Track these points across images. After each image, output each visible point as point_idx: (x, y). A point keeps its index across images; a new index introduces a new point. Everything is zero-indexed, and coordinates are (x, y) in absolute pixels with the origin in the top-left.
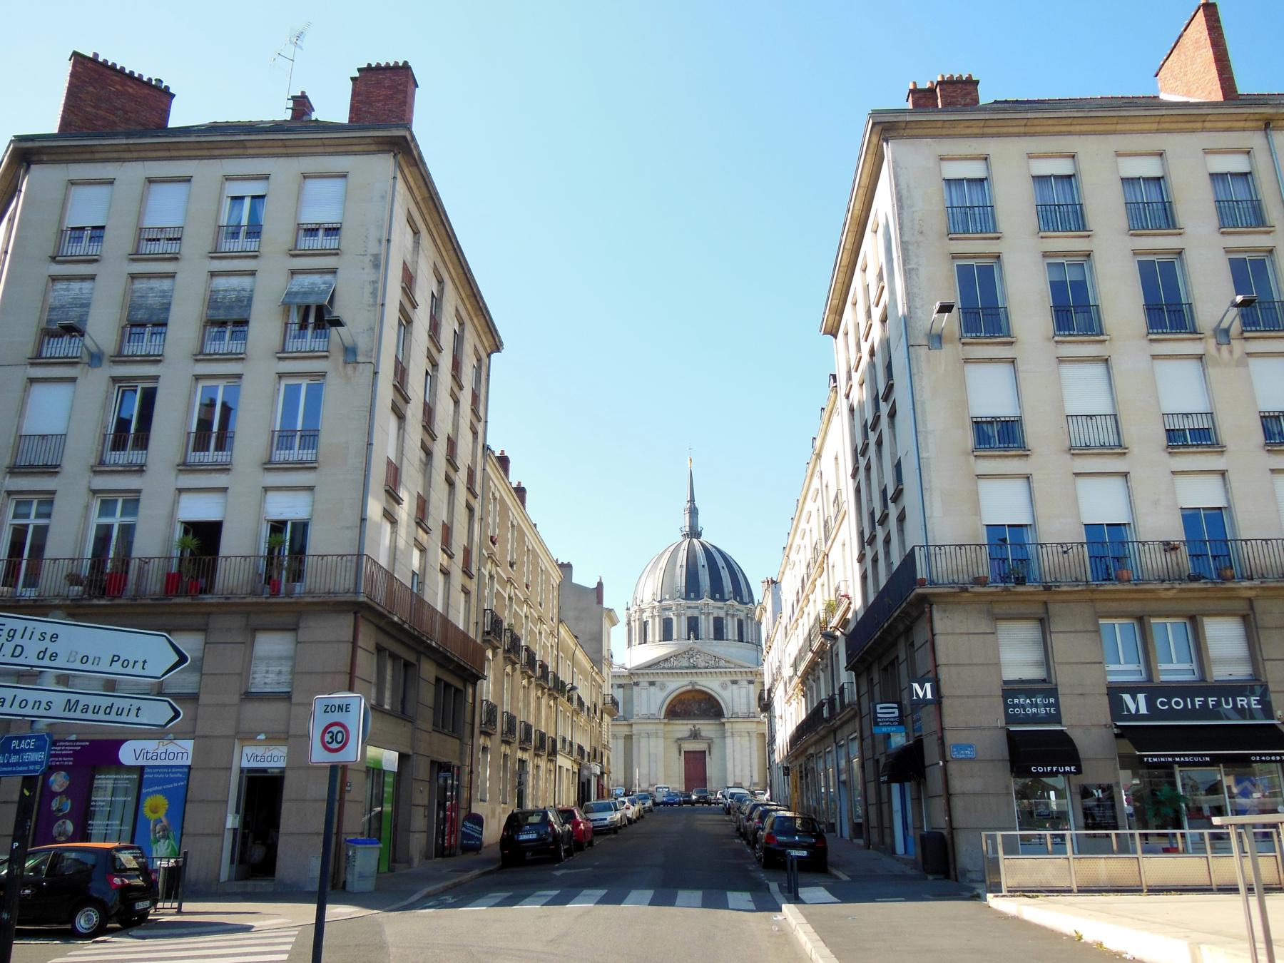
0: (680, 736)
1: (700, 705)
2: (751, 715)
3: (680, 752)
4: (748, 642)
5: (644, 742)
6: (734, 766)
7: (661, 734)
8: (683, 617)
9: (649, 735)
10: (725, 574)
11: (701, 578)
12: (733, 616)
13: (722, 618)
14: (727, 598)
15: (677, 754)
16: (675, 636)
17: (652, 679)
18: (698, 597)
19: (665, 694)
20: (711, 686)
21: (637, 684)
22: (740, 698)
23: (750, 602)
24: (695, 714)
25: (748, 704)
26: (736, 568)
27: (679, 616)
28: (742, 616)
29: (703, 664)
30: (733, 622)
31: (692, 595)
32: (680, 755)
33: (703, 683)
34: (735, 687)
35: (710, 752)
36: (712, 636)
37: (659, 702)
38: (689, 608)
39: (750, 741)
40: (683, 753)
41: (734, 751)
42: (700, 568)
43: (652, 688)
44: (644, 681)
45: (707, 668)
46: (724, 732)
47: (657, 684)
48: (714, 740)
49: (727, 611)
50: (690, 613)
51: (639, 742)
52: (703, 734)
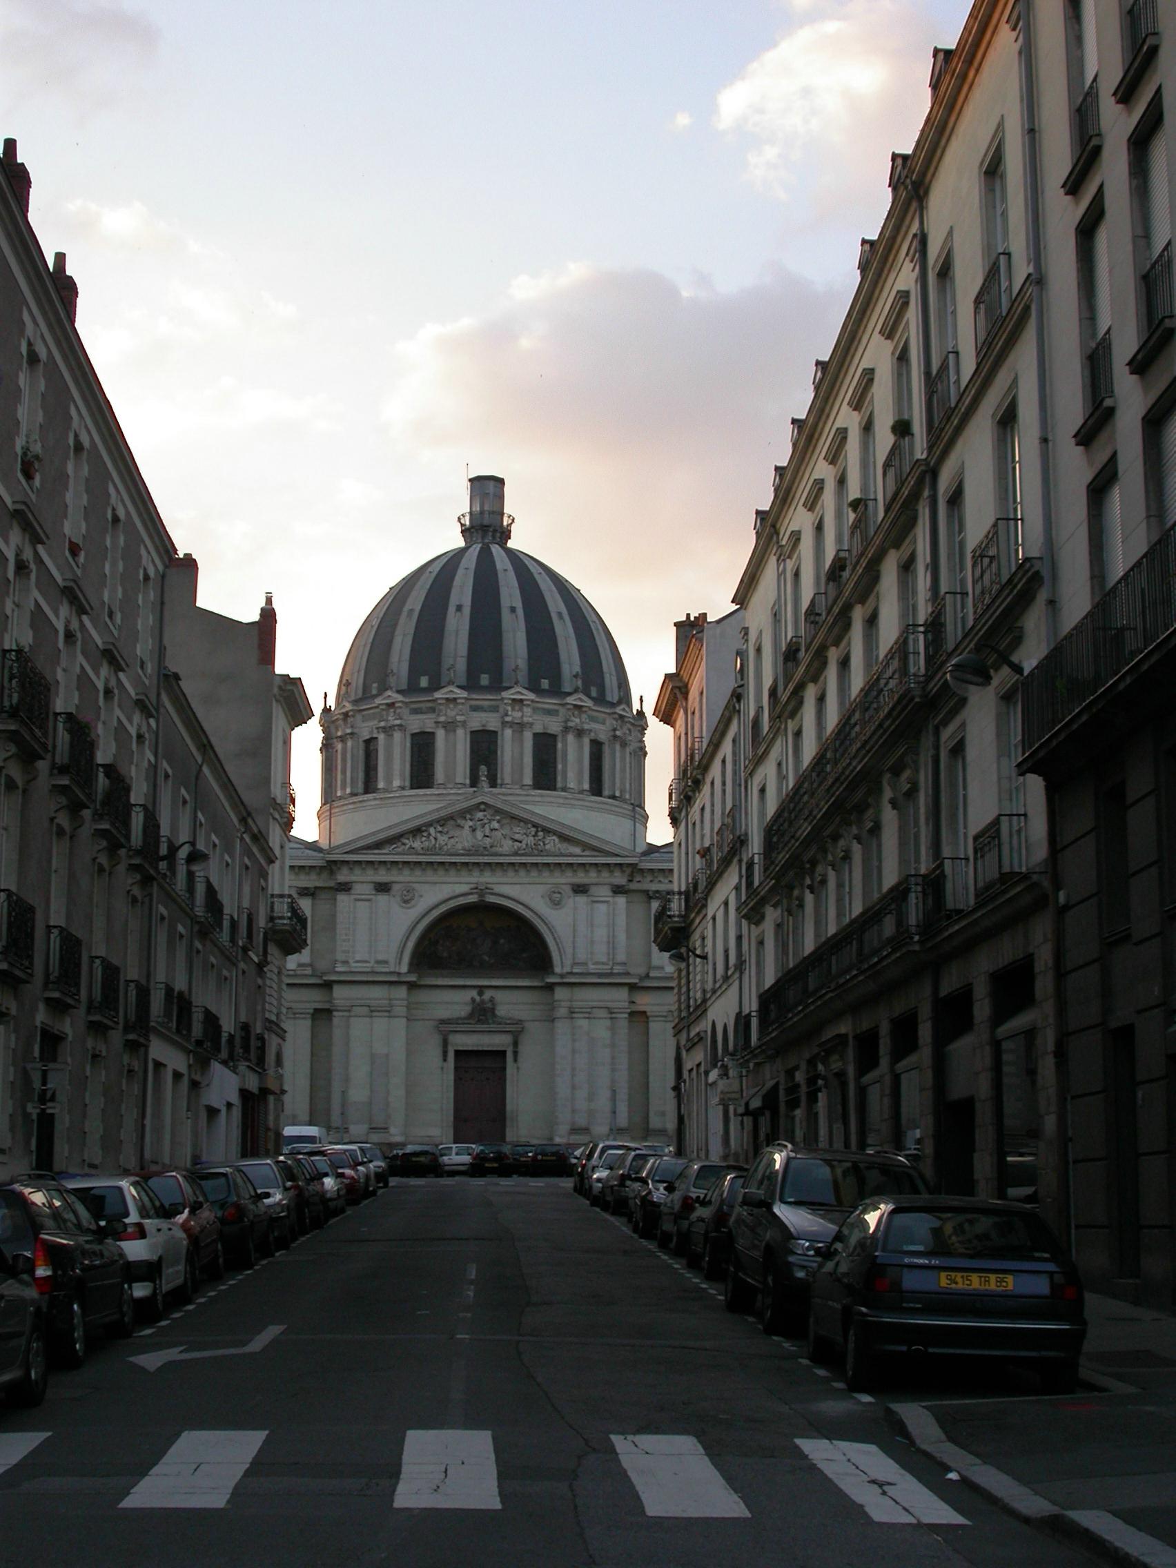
0: (444, 1013)
2: (617, 969)
3: (445, 1053)
4: (613, 797)
5: (358, 1026)
6: (574, 1087)
7: (401, 1011)
8: (460, 732)
9: (373, 1011)
10: (564, 631)
11: (507, 637)
12: (580, 733)
13: (554, 737)
14: (568, 690)
15: (438, 1052)
16: (440, 775)
17: (382, 876)
18: (497, 685)
20: (523, 898)
21: (345, 888)
22: (591, 925)
23: (620, 702)
25: (612, 943)
26: (591, 618)
28: (602, 731)
29: (507, 846)
30: (581, 747)
31: (485, 680)
32: (445, 1060)
33: (506, 890)
34: (581, 900)
36: (528, 779)
37: (400, 930)
38: (475, 709)
39: (612, 1029)
40: (451, 1055)
41: (574, 1051)
43: (382, 899)
44: (363, 881)
45: (516, 854)
46: (552, 1007)
47: (396, 887)
48: (526, 1025)
49: (567, 721)
50: (477, 721)
51: (348, 1027)
52: (501, 1011)
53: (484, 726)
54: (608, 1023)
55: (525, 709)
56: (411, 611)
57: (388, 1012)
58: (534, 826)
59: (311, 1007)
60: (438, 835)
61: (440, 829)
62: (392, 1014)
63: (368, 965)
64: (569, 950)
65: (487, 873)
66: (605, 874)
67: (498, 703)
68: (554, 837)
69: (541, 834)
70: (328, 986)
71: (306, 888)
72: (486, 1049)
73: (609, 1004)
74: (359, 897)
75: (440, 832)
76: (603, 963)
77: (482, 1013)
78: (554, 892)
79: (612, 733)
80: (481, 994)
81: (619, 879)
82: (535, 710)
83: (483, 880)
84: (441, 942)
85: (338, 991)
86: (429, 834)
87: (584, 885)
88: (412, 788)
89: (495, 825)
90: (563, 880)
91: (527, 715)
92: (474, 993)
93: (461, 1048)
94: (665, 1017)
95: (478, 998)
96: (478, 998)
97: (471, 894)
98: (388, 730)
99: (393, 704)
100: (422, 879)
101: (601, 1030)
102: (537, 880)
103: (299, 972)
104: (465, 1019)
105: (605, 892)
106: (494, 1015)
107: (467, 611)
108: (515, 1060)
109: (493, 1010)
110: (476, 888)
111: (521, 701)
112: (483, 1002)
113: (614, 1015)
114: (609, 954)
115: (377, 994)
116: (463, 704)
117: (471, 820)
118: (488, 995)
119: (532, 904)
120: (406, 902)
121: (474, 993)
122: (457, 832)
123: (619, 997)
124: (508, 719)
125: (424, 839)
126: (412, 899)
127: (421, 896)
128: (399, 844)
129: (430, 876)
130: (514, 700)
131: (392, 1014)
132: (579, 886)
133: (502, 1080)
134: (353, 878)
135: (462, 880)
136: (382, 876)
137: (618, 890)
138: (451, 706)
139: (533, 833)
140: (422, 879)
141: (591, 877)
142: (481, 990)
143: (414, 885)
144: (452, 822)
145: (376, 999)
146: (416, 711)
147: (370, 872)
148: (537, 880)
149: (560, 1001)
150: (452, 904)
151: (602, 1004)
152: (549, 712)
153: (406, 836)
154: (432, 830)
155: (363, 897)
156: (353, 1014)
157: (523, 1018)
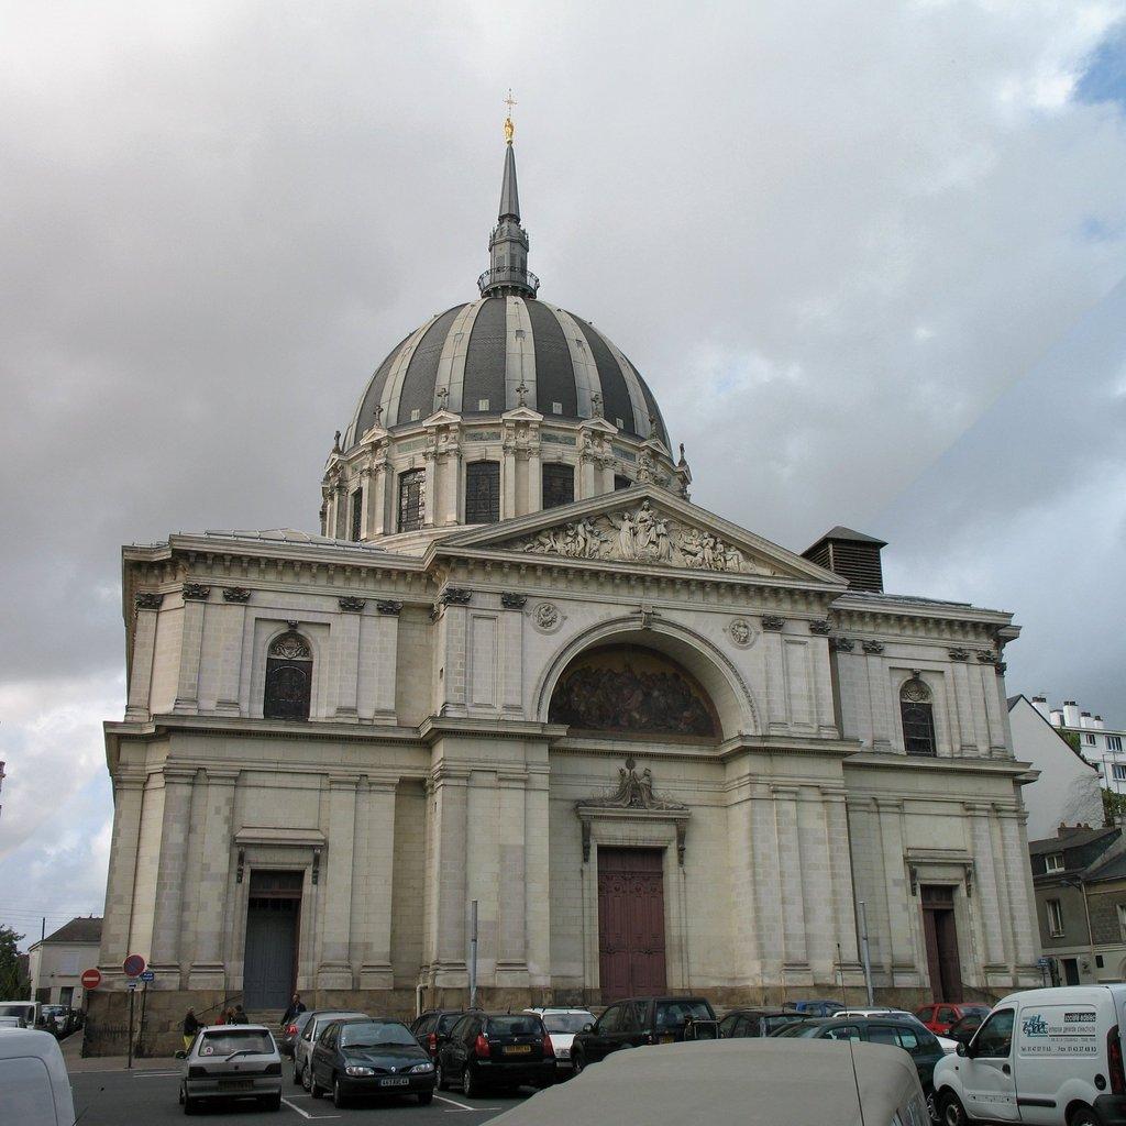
0: (584, 792)
1: (647, 695)
6: (783, 902)
7: (541, 781)
9: (504, 779)
15: (577, 848)
17: (513, 585)
20: (700, 630)
22: (787, 673)
24: (632, 724)
31: (557, 408)
32: (586, 860)
34: (774, 638)
35: (681, 851)
38: (547, 438)
42: (573, 346)
43: (513, 618)
51: (466, 802)
52: (661, 790)
54: (819, 808)
55: (606, 445)
57: (526, 785)
59: (395, 775)
60: (588, 535)
61: (589, 528)
63: (491, 711)
64: (763, 706)
65: (654, 594)
66: (801, 607)
68: (738, 552)
69: (720, 546)
70: (427, 744)
71: (391, 603)
72: (640, 844)
73: (822, 782)
75: (591, 532)
76: (805, 725)
77: (635, 793)
78: (739, 626)
80: (630, 765)
81: (818, 613)
83: (645, 601)
84: (576, 689)
85: (441, 750)
88: (467, 523)
89: (661, 529)
91: (606, 451)
93: (606, 843)
94: (867, 805)
95: (627, 771)
96: (627, 771)
97: (633, 619)
98: (438, 457)
99: (447, 426)
101: (815, 819)
103: (376, 722)
104: (615, 799)
105: (802, 629)
106: (651, 797)
107: (530, 336)
108: (681, 862)
109: (649, 787)
111: (603, 433)
112: (634, 777)
113: (826, 798)
114: (811, 712)
115: (508, 754)
116: (536, 430)
119: (712, 639)
120: (544, 624)
121: (622, 764)
123: (831, 772)
124: (589, 451)
125: (569, 539)
126: (552, 621)
127: (565, 618)
128: (536, 543)
129: (577, 591)
130: (594, 431)
131: (529, 786)
132: (769, 618)
133: (658, 891)
134: (473, 586)
135: (621, 599)
136: (513, 585)
137: (817, 629)
139: (711, 544)
140: (565, 594)
141: (783, 609)
142: (631, 758)
143: (554, 602)
144: (605, 521)
145: (510, 762)
146: (475, 437)
148: (715, 608)
151: (811, 782)
152: (627, 455)
154: (580, 528)
155: (484, 613)
157: (688, 803)
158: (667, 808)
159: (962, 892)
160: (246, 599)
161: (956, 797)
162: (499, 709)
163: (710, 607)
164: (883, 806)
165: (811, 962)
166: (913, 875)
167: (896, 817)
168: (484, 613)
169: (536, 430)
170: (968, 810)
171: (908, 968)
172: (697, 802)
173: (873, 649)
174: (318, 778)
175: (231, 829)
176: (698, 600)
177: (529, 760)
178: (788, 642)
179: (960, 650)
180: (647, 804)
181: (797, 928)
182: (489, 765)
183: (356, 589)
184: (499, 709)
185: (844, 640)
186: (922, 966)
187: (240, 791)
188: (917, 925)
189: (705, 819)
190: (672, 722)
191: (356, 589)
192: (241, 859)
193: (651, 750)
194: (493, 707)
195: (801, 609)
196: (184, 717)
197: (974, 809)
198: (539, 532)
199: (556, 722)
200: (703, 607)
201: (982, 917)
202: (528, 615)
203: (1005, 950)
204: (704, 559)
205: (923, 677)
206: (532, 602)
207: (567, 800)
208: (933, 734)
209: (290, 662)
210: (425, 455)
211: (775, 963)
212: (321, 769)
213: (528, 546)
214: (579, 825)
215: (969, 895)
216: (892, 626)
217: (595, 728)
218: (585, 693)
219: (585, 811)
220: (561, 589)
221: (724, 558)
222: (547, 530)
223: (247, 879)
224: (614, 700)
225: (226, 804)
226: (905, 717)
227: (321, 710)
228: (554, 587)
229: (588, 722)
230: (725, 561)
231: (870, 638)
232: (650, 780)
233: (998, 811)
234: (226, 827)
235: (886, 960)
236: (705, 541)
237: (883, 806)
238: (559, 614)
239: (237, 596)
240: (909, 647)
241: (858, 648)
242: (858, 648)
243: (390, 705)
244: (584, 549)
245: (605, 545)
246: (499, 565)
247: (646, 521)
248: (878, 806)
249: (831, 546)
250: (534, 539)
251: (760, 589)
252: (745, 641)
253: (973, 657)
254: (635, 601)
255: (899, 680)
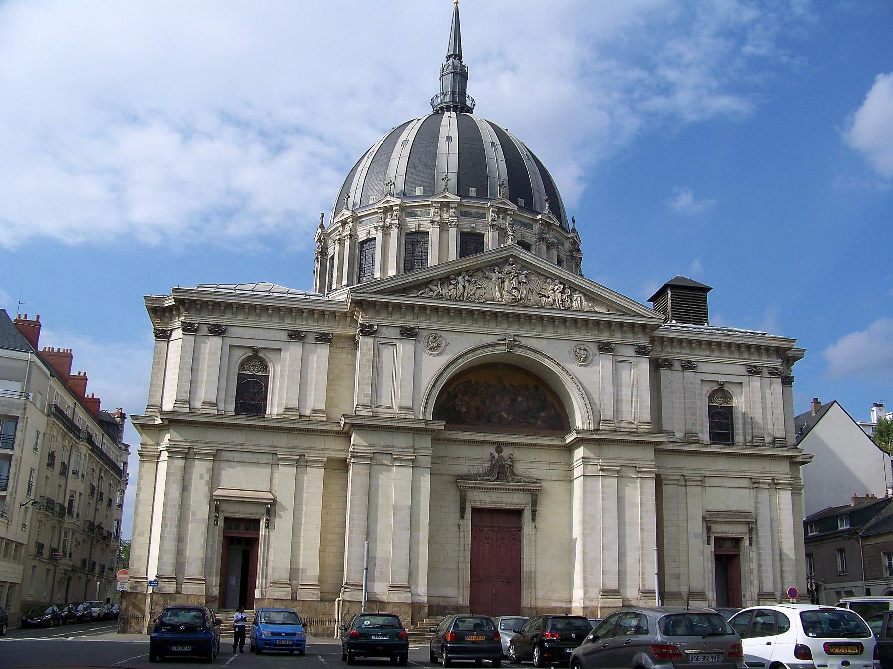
0: (464, 470)
7: (426, 461)
15: (455, 509)
17: (409, 321)
19: (441, 361)
27: (443, 227)
29: (534, 298)
31: (473, 192)
32: (462, 517)
38: (464, 214)
42: (488, 147)
44: (389, 324)
52: (521, 468)
53: (473, 228)
56: (407, 141)
58: (561, 284)
60: (467, 284)
61: (467, 278)
62: (417, 465)
67: (486, 211)
68: (581, 295)
69: (568, 292)
72: (504, 507)
74: (383, 341)
75: (468, 281)
76: (628, 422)
78: (580, 349)
79: (568, 254)
82: (515, 222)
83: (508, 331)
84: (460, 396)
86: (458, 283)
87: (609, 344)
90: (589, 338)
92: (492, 450)
93: (478, 506)
94: (678, 480)
95: (496, 455)
96: (496, 455)
97: (499, 345)
99: (392, 206)
100: (448, 327)
102: (564, 336)
103: (314, 419)
104: (485, 474)
106: (513, 474)
107: (455, 141)
108: (534, 520)
110: (505, 339)
112: (501, 459)
115: (401, 441)
117: (499, 273)
118: (506, 453)
122: (485, 283)
125: (452, 287)
129: (458, 325)
130: (499, 208)
135: (490, 330)
136: (409, 321)
137: (641, 351)
138: (445, 209)
140: (448, 327)
141: (615, 338)
142: (499, 446)
144: (481, 274)
146: (413, 215)
147: (396, 317)
149: (589, 458)
150: (479, 354)
152: (525, 225)
153: (435, 283)
156: (374, 462)
158: (524, 482)
159: (746, 542)
160: (223, 332)
161: (746, 474)
162: (396, 410)
163: (558, 336)
164: (690, 480)
165: (621, 590)
166: (709, 529)
167: (699, 489)
168: (387, 341)
169: (456, 208)
170: (754, 483)
171: (701, 595)
172: (548, 478)
173: (688, 366)
174: (270, 457)
175: (211, 490)
176: (550, 332)
177: (417, 446)
178: (618, 361)
179: (755, 367)
180: (510, 479)
181: (614, 567)
182: (387, 449)
183: (300, 325)
184: (396, 410)
185: (666, 360)
186: (711, 594)
187: (217, 463)
188: (710, 565)
189: (553, 489)
190: (532, 421)
191: (300, 325)
192: (217, 509)
193: (513, 440)
194: (392, 408)
195: (630, 338)
196: (178, 413)
197: (759, 483)
198: (430, 282)
199: (438, 419)
200: (553, 335)
201: (759, 560)
202: (420, 342)
203: (775, 583)
204: (554, 300)
205: (729, 388)
206: (424, 333)
207: (452, 475)
208: (733, 429)
209: (254, 376)
210: (376, 228)
211: (595, 592)
212: (272, 450)
213: (421, 292)
214: (459, 493)
215: (750, 544)
216: (704, 350)
217: (473, 424)
218: (466, 398)
219: (462, 482)
220: (445, 323)
221: (571, 299)
222: (435, 280)
223: (221, 523)
224: (488, 403)
225: (207, 473)
226: (712, 416)
227: (274, 408)
228: (439, 322)
229: (467, 420)
230: (571, 301)
231: (686, 358)
232: (512, 462)
233: (776, 484)
234: (207, 487)
235: (684, 590)
236: (556, 287)
237: (690, 480)
238: (443, 342)
239: (217, 330)
240: (717, 365)
241: (677, 366)
242: (677, 366)
243: (323, 407)
244: (463, 294)
245: (480, 290)
246: (399, 307)
247: (511, 272)
248: (686, 481)
249: (669, 292)
250: (426, 287)
251: (598, 323)
252: (584, 361)
253: (765, 372)
254: (501, 331)
255: (707, 389)
